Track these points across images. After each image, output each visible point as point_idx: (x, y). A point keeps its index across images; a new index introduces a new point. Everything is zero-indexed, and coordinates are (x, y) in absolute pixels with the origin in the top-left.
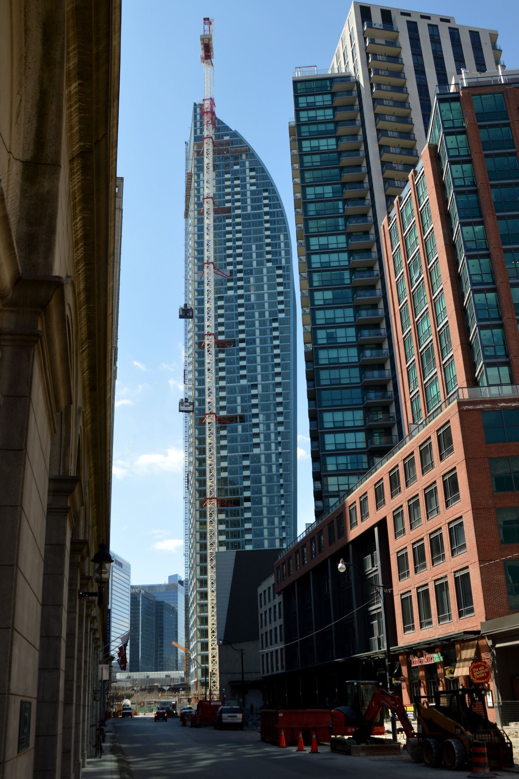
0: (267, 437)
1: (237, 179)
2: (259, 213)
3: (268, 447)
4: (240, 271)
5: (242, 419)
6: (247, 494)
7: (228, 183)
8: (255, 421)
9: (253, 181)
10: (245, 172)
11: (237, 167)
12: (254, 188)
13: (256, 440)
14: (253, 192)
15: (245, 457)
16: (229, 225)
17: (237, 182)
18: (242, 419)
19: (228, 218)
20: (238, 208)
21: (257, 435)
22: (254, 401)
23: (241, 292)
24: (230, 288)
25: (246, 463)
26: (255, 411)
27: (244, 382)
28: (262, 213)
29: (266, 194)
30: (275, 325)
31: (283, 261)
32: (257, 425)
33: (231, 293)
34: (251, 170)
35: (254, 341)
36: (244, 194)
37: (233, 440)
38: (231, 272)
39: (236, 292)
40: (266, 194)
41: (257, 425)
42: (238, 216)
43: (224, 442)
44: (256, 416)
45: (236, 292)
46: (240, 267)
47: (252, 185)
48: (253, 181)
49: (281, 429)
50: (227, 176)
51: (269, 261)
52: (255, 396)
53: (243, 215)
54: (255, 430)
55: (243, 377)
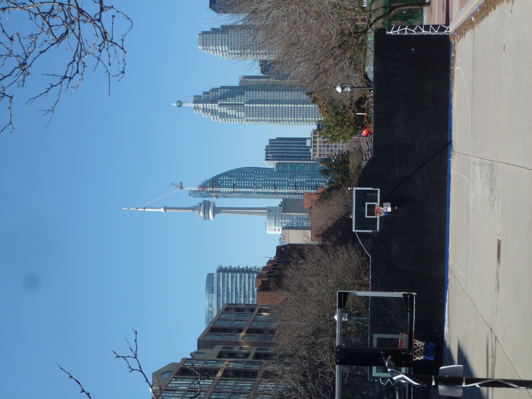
0: (301, 178)
1: (223, 182)
3: (304, 178)
4: (254, 182)
5: (296, 184)
6: (315, 183)
7: (225, 184)
8: (297, 181)
9: (225, 177)
10: (221, 180)
11: (219, 182)
12: (227, 177)
13: (302, 181)
14: (228, 178)
15: (306, 183)
16: (239, 185)
17: (225, 182)
18: (296, 184)
19: (236, 185)
20: (233, 182)
21: (300, 180)
22: (292, 180)
23: (260, 183)
24: (259, 185)
25: (307, 183)
26: (294, 180)
27: (286, 183)
29: (230, 174)
30: (271, 174)
31: (252, 171)
32: (298, 180)
33: (260, 185)
34: (221, 178)
35: (275, 180)
36: (229, 180)
37: (301, 187)
40: (230, 174)
41: (298, 180)
42: (236, 182)
43: (302, 188)
44: (295, 180)
46: (253, 182)
47: (226, 178)
48: (225, 177)
49: (299, 174)
50: (222, 185)
51: (251, 175)
52: (290, 180)
54: (299, 181)
55: (285, 183)
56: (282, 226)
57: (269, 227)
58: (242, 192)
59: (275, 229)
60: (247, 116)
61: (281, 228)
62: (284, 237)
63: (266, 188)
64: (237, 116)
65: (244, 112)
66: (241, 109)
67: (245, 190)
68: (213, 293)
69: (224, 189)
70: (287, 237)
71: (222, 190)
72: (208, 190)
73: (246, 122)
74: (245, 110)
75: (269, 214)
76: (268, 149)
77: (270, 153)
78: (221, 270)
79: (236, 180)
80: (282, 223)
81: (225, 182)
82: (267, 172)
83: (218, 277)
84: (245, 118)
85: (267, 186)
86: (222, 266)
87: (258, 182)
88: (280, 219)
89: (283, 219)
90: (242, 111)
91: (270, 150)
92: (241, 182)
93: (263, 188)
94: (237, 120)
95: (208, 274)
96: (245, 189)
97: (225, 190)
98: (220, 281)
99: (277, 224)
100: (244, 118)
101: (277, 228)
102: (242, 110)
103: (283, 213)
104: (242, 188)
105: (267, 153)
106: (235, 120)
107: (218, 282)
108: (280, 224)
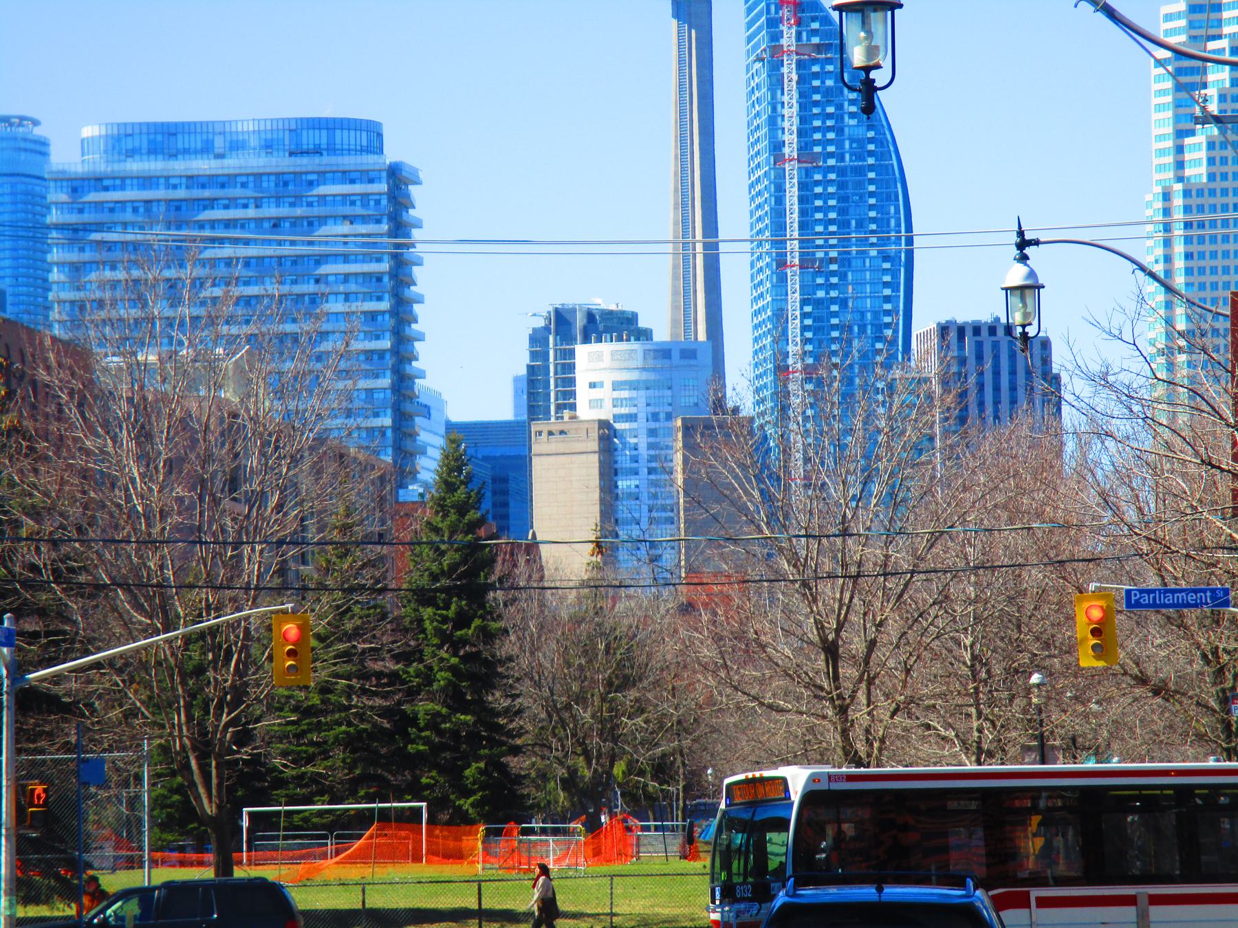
1: (829, 103)
2: (861, 166)
4: (832, 260)
20: (831, 155)
23: (834, 294)
28: (864, 166)
38: (821, 260)
39: (827, 293)
42: (831, 169)
45: (827, 293)
53: (839, 167)
56: (617, 418)
57: (607, 361)
58: (780, 200)
59: (601, 385)
60: (1187, 193)
61: (606, 414)
62: (562, 432)
63: (808, 322)
64: (1188, 141)
65: (1212, 177)
66: (1224, 161)
67: (793, 218)
68: (291, 154)
69: (796, 107)
70: (562, 447)
71: (786, 99)
72: (784, 28)
73: (1159, 189)
74: (1219, 185)
75: (676, 354)
76: (1001, 332)
77: (979, 345)
78: (398, 178)
79: (841, 172)
80: (631, 418)
81: (831, 110)
82: (888, 325)
83: (368, 177)
84: (1179, 187)
85: (816, 330)
86: (417, 182)
87: (834, 280)
88: (651, 409)
89: (653, 425)
90: (1214, 169)
91: (996, 346)
92: (831, 196)
93: (808, 309)
94: (1169, 143)
95: (380, 124)
96: (796, 215)
97: (786, 112)
98: (352, 181)
99: (625, 394)
100: (1180, 179)
101: (606, 393)
102: (1218, 169)
103: (679, 423)
104: (801, 200)
105: (977, 329)
106: (1169, 129)
107: (344, 172)
108: (624, 410)
